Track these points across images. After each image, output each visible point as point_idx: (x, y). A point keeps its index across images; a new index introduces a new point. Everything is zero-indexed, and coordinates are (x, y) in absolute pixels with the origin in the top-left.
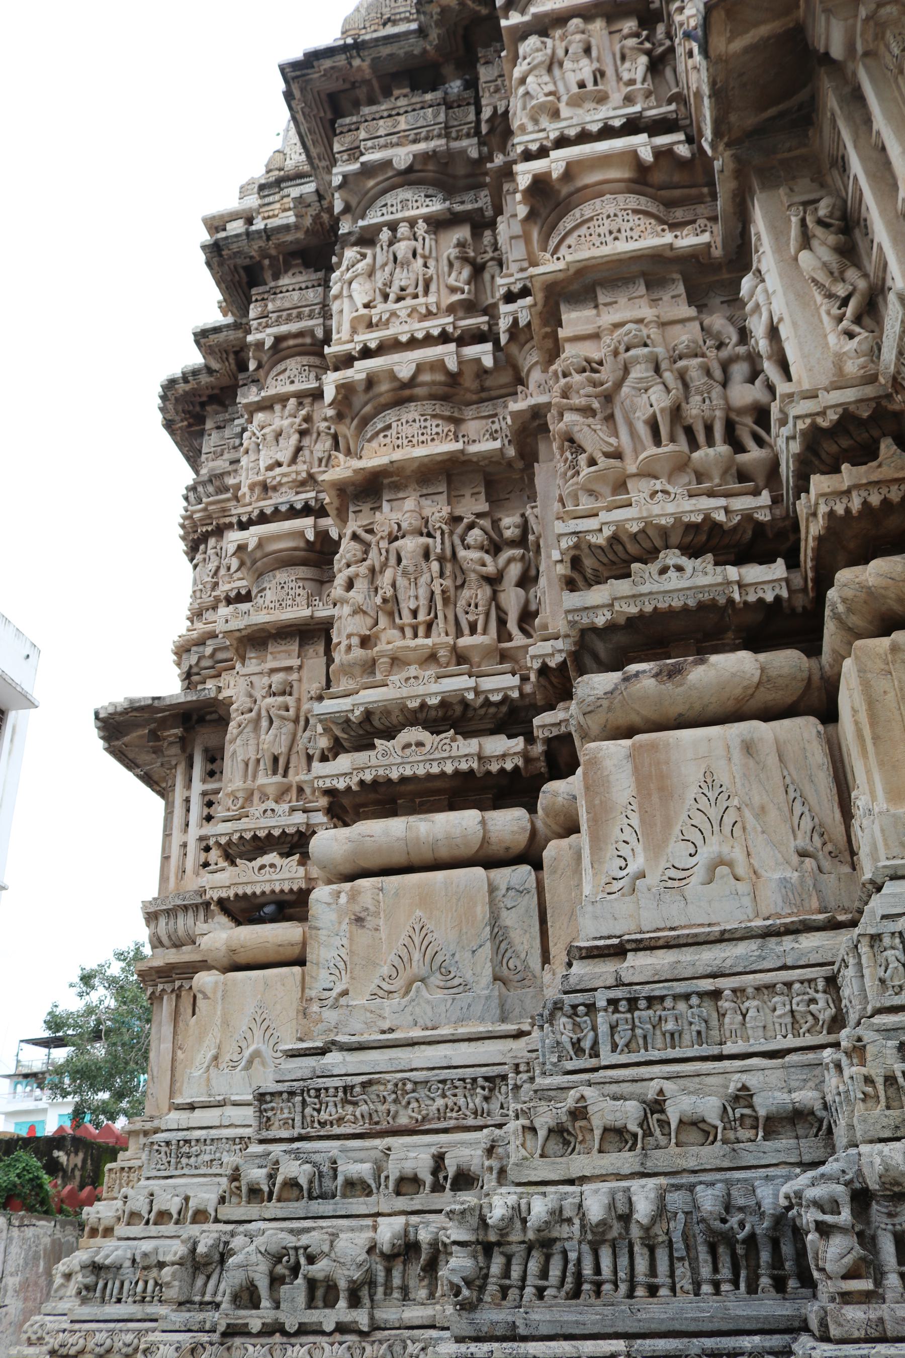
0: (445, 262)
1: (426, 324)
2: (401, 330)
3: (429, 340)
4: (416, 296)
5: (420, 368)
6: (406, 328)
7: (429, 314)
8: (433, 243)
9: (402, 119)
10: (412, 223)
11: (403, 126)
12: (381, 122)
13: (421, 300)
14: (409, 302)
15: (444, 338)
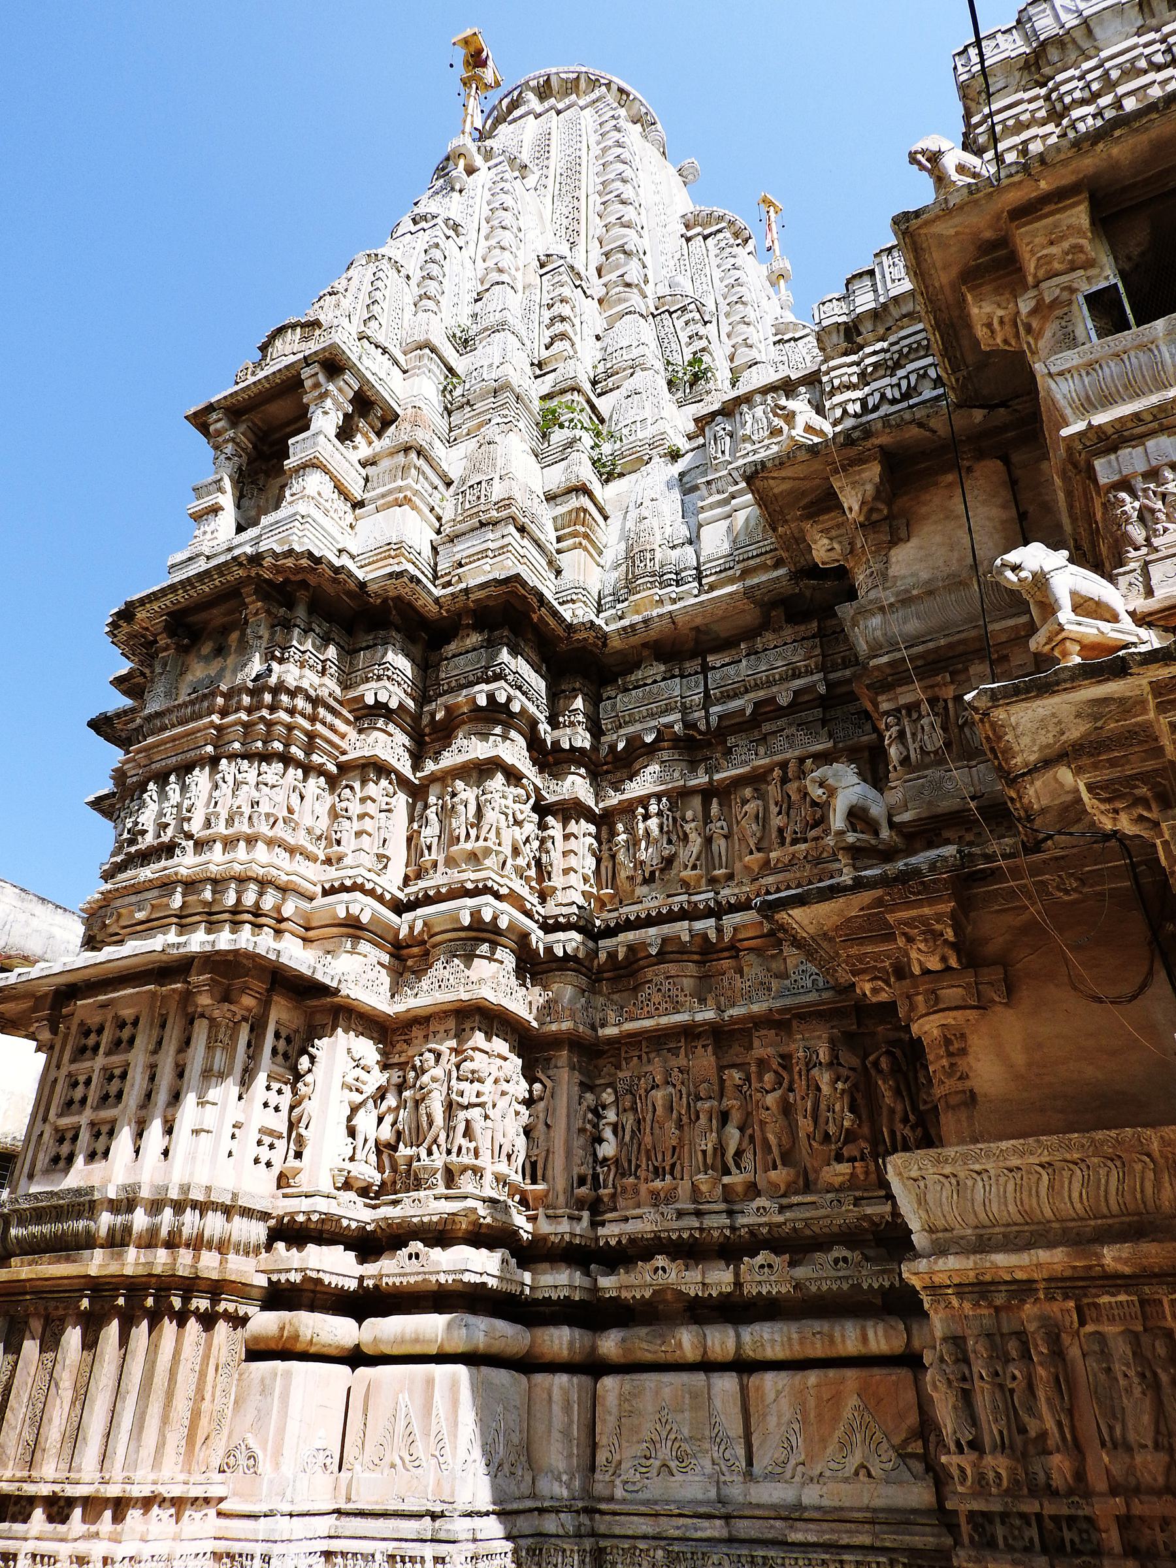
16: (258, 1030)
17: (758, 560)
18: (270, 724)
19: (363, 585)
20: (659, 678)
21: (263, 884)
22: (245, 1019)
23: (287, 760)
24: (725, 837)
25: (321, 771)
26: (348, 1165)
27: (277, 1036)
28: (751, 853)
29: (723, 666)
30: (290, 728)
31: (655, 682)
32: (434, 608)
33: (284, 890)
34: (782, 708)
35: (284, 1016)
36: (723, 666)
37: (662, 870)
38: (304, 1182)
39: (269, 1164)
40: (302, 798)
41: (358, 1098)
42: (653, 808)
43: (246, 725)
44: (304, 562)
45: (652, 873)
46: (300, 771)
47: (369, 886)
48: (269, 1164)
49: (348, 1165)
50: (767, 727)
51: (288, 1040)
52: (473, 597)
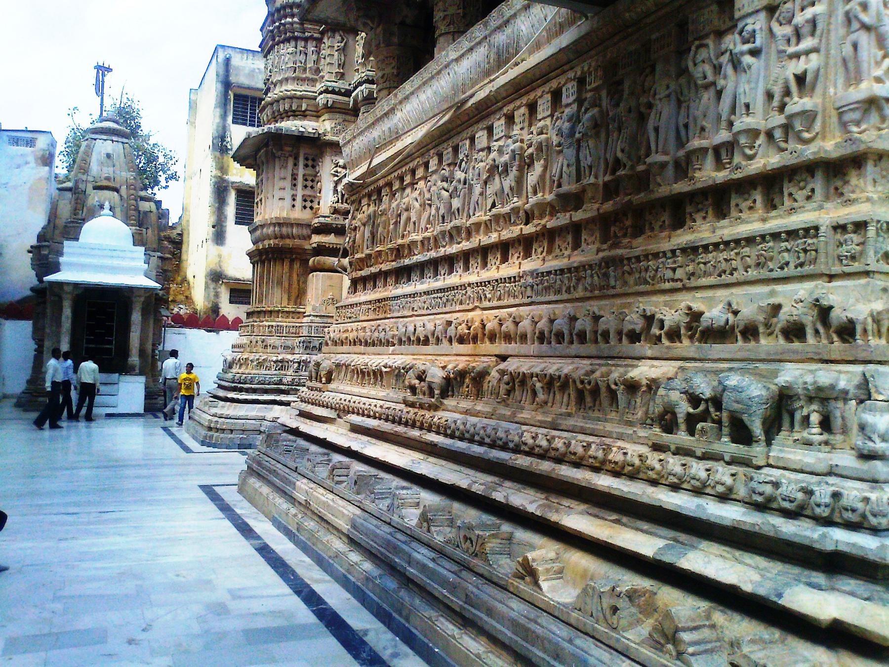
16: (296, 158)
18: (284, 25)
21: (291, 98)
22: (291, 156)
23: (296, 39)
25: (312, 38)
26: (335, 205)
27: (307, 159)
30: (292, 24)
33: (301, 98)
35: (308, 151)
38: (321, 213)
39: (311, 208)
40: (306, 54)
41: (336, 179)
43: (278, 27)
46: (303, 43)
47: (330, 89)
48: (311, 208)
49: (335, 205)
51: (313, 160)
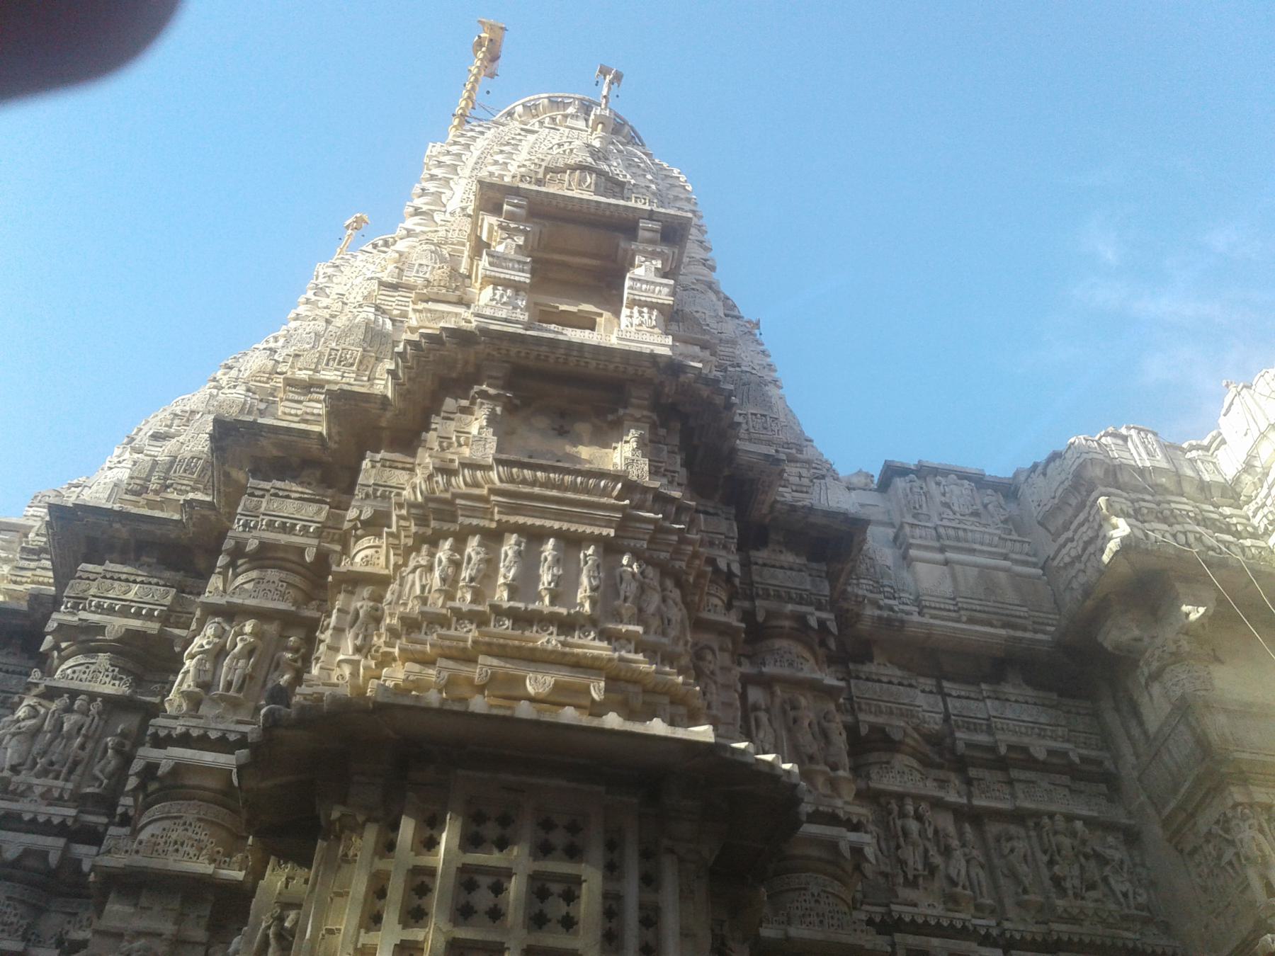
0: (103, 746)
1: (52, 810)
2: (26, 808)
3: (46, 828)
4: (57, 778)
5: (27, 853)
6: (33, 807)
7: (59, 801)
8: (102, 723)
9: (136, 588)
10: (92, 696)
11: (131, 596)
12: (116, 584)
13: (60, 783)
14: (49, 781)
15: (61, 829)
17: (984, 616)
19: (734, 451)
20: (895, 680)
24: (982, 867)
28: (1025, 891)
29: (959, 697)
31: (890, 682)
32: (765, 510)
34: (1035, 761)
36: (959, 697)
37: (924, 877)
42: (910, 808)
44: (719, 400)
45: (915, 877)
50: (1015, 773)
52: (812, 519)
